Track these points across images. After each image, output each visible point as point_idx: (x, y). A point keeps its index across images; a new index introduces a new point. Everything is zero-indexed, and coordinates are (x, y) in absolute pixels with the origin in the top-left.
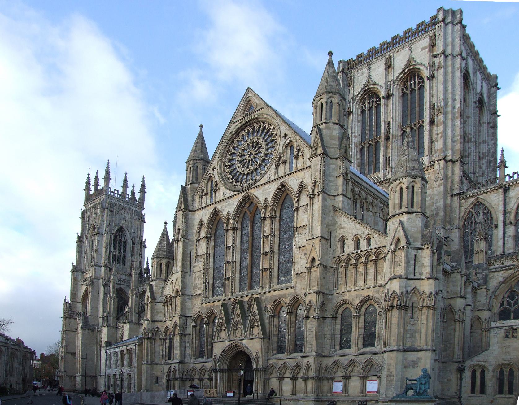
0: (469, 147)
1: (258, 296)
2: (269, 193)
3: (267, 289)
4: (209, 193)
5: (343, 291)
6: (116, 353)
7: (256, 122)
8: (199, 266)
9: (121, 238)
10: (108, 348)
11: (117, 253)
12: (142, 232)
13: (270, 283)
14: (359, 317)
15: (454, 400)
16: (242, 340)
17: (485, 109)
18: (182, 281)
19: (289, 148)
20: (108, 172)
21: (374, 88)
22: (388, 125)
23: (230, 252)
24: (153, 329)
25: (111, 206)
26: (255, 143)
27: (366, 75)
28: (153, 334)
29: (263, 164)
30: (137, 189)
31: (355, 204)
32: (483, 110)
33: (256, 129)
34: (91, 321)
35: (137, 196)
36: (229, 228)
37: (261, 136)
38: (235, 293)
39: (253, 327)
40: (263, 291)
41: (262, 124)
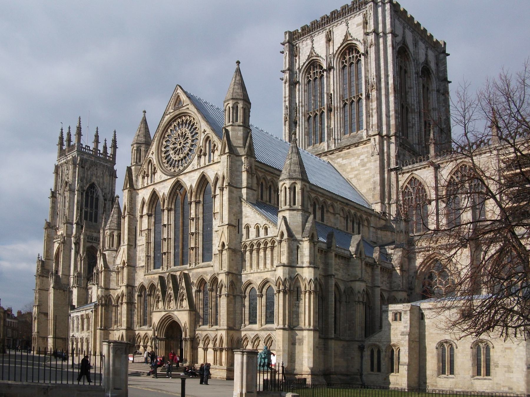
0: (413, 118)
1: (186, 272)
2: (193, 180)
3: (193, 266)
4: (150, 175)
5: (249, 272)
6: (77, 317)
7: (185, 116)
8: (141, 240)
9: (93, 194)
10: (72, 312)
11: (89, 210)
12: (113, 188)
13: (196, 260)
14: (261, 296)
15: (356, 376)
16: (174, 311)
17: (433, 76)
18: (128, 254)
19: (208, 142)
20: (79, 129)
21: (317, 59)
22: (330, 96)
23: (165, 230)
24: (106, 296)
25: (82, 162)
26: (184, 134)
27: (310, 46)
28: (106, 301)
29: (190, 153)
30: (109, 144)
31: (268, 191)
32: (431, 78)
33: (184, 121)
34: (64, 281)
35: (110, 151)
36: (165, 208)
37: (188, 128)
38: (170, 267)
39: (182, 300)
40: (191, 267)
41: (188, 118)
